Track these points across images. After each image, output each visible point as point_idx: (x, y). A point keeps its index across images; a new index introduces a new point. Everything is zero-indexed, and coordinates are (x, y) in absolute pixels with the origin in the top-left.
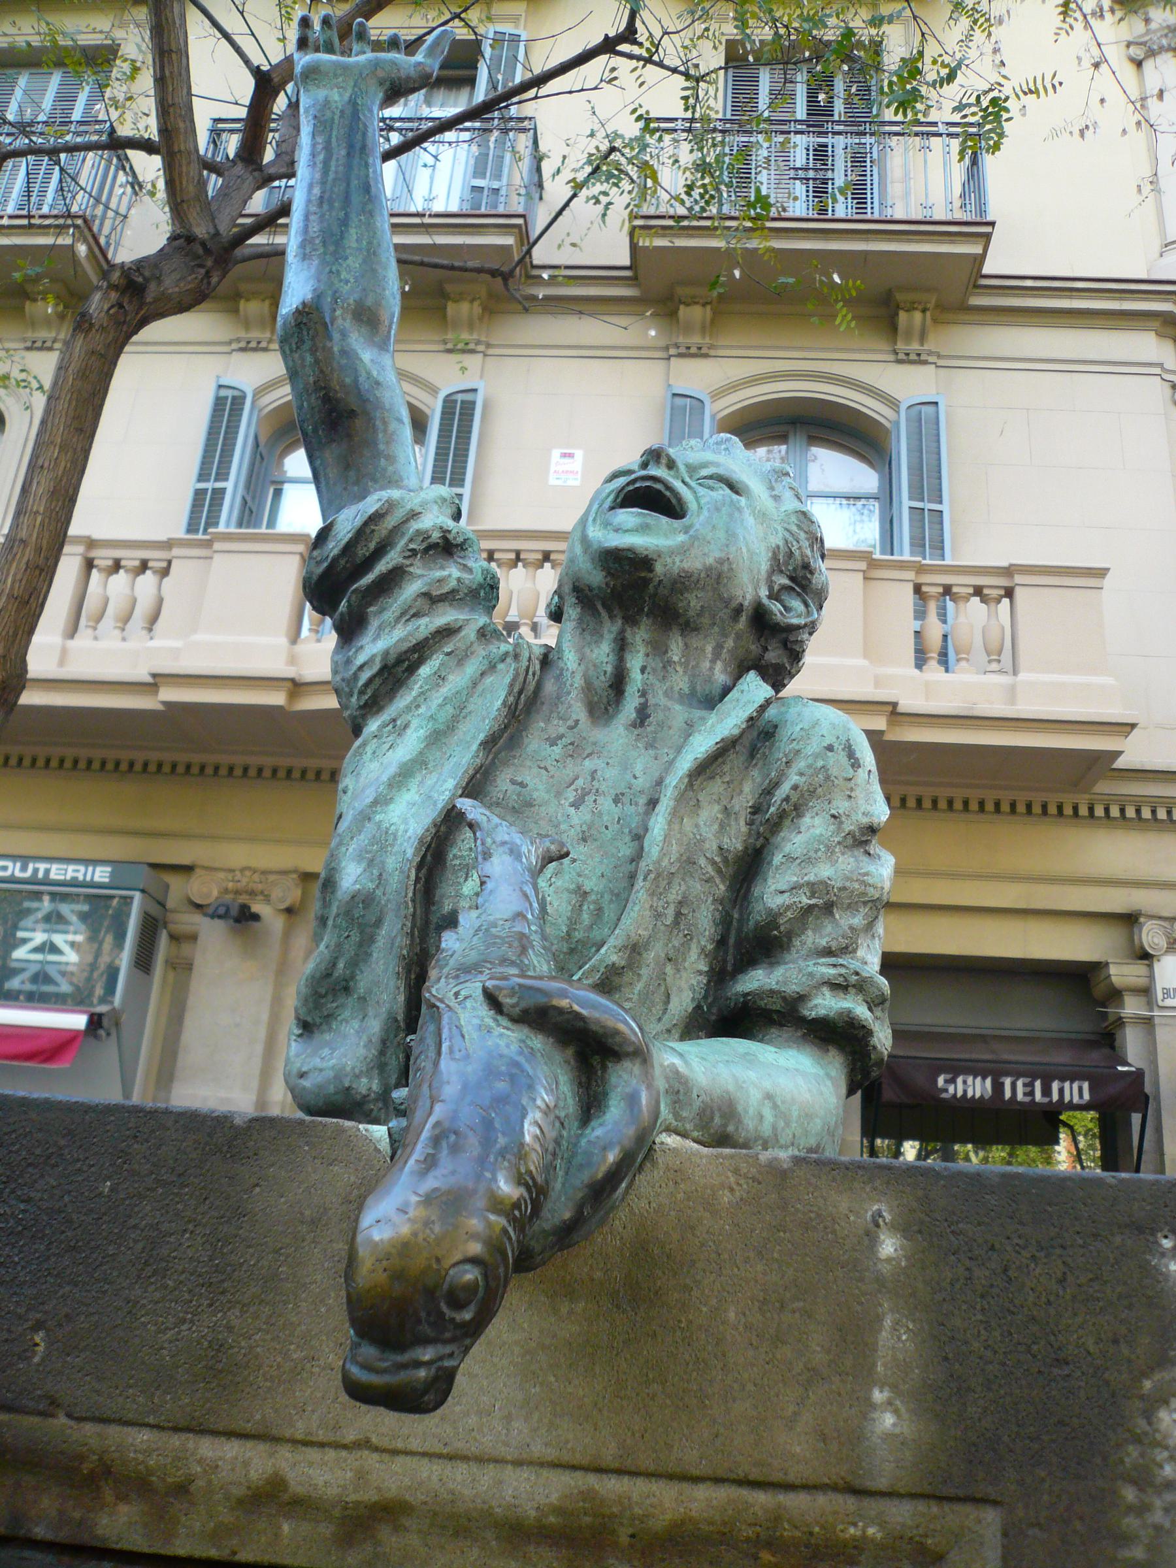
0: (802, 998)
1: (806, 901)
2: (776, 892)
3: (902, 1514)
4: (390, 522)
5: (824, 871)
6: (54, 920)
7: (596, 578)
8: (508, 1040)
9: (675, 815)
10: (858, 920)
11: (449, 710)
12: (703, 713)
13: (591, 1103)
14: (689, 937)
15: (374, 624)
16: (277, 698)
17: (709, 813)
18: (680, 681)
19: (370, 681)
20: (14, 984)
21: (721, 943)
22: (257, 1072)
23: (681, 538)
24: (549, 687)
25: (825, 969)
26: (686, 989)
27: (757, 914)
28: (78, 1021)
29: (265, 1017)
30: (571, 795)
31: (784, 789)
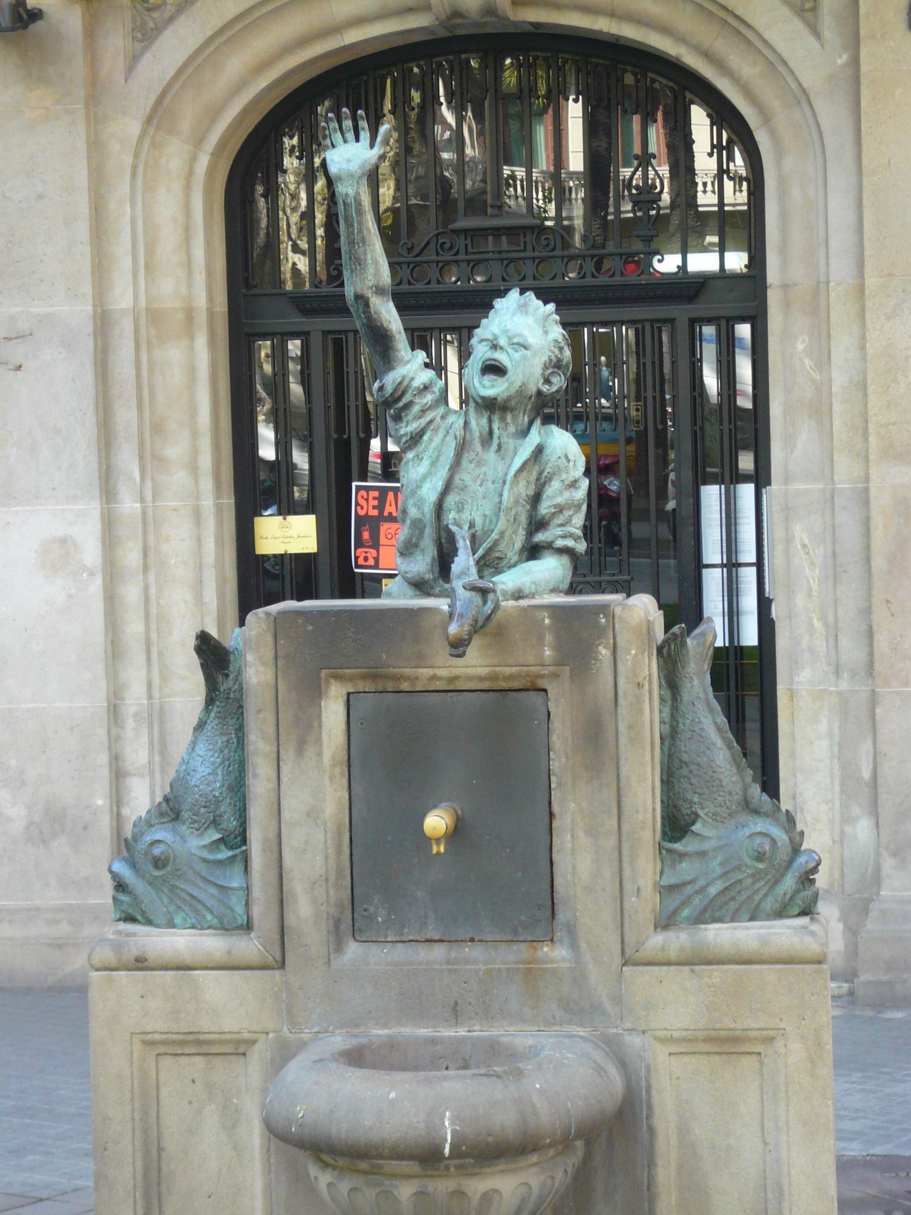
0: (552, 542)
1: (553, 511)
2: (544, 508)
3: (551, 669)
4: (405, 383)
5: (559, 500)
7: (479, 401)
8: (468, 594)
9: (511, 488)
10: (571, 513)
11: (436, 453)
12: (519, 442)
13: (485, 602)
14: (519, 525)
15: (405, 420)
17: (522, 483)
18: (512, 429)
19: (407, 441)
21: (530, 524)
22: (87, 268)
23: (506, 385)
24: (468, 436)
25: (559, 532)
26: (519, 541)
27: (539, 517)
29: (82, 178)
30: (479, 482)
31: (546, 473)
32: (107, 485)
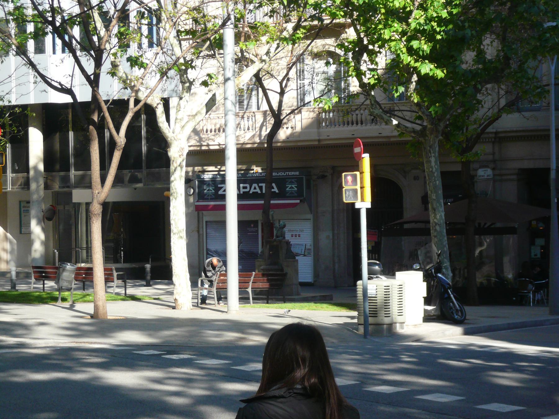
6: (292, 183)
16: (317, 143)
20: (287, 195)
28: (298, 201)
32: (333, 230)
